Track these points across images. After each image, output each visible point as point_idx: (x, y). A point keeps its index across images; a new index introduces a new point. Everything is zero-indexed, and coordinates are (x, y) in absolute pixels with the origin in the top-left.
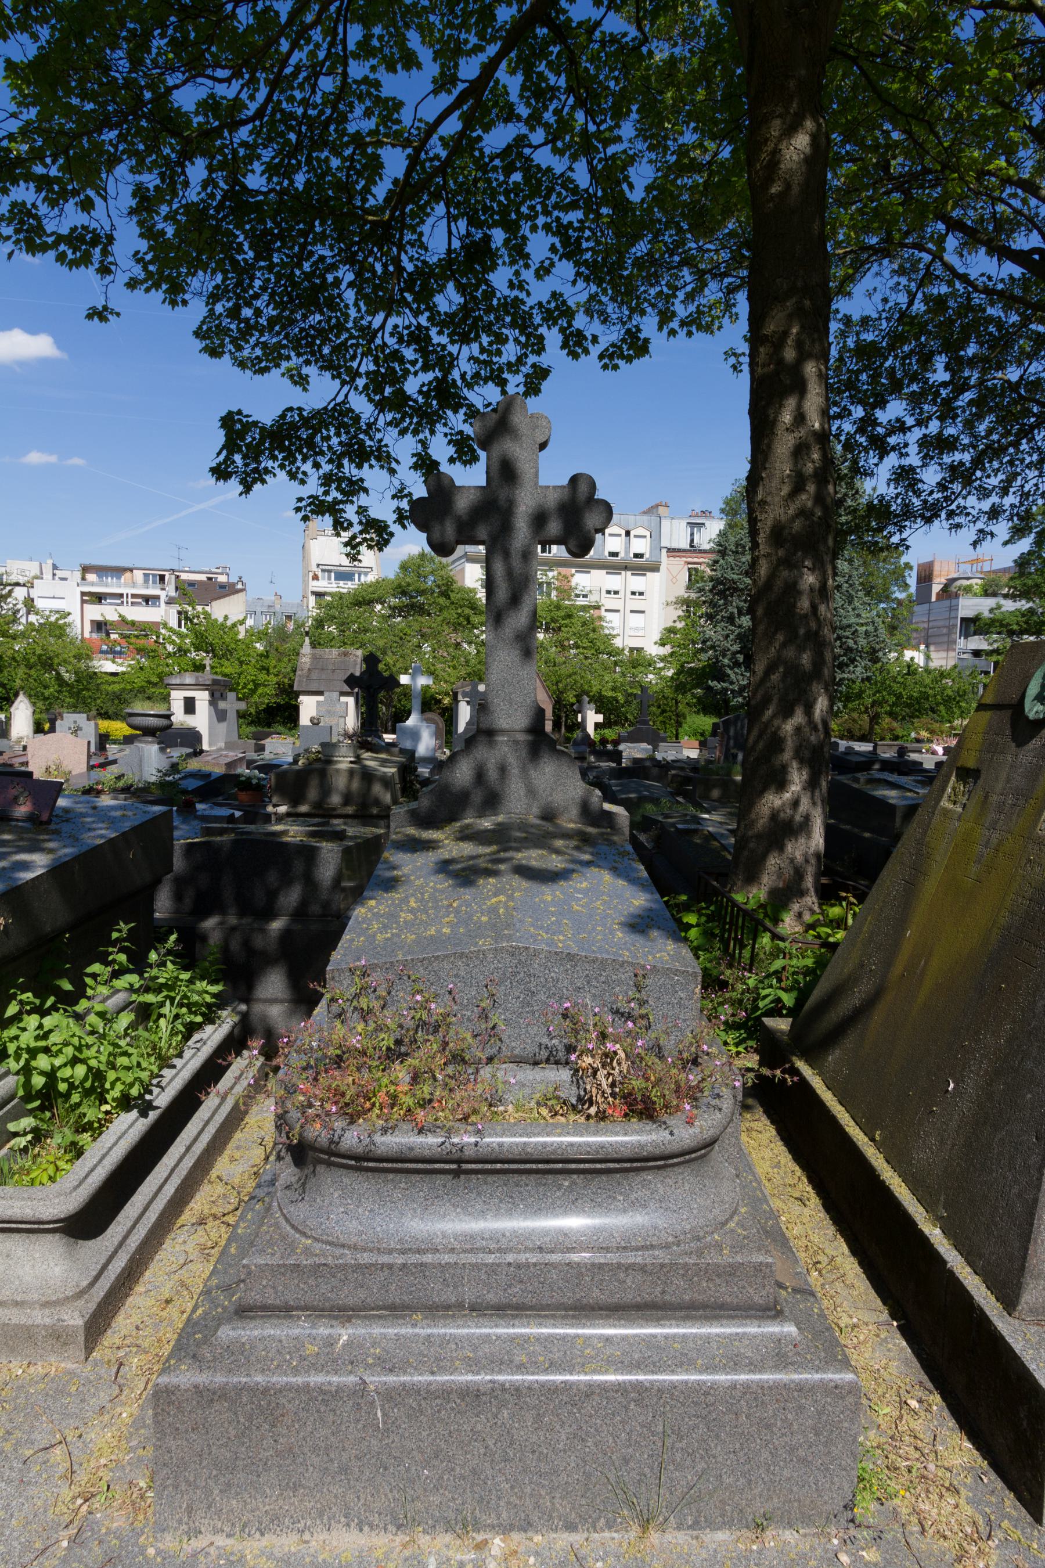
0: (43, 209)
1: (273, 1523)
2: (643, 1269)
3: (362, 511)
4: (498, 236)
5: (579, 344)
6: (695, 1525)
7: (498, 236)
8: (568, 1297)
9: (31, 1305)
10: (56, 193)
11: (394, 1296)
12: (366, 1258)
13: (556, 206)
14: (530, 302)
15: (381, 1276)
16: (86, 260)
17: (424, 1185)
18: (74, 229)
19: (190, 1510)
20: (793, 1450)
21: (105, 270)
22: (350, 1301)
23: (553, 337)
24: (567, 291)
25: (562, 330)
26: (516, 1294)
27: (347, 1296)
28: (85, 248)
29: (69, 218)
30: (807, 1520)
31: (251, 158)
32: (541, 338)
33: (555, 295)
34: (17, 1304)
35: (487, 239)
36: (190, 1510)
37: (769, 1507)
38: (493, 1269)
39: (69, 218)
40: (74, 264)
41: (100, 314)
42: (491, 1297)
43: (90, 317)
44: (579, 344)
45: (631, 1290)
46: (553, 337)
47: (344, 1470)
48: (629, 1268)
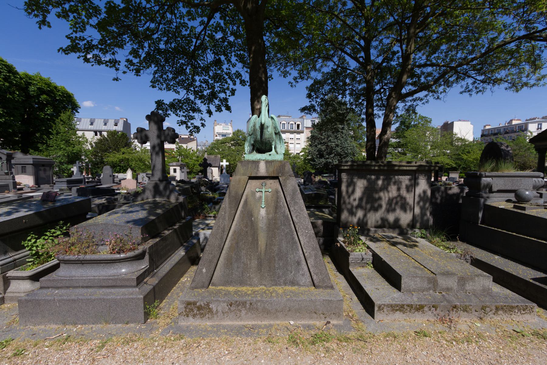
0: (101, 55)
1: (40, 323)
2: (112, 279)
3: (192, 124)
4: (223, 58)
5: (244, 83)
6: (115, 323)
7: (223, 58)
8: (99, 285)
9: (21, 293)
10: (105, 52)
11: (67, 285)
12: (63, 278)
13: (237, 50)
14: (232, 73)
15: (65, 281)
16: (114, 66)
17: (76, 266)
18: (110, 59)
19: (25, 322)
20: (132, 309)
21: (117, 69)
22: (60, 286)
23: (238, 81)
24: (240, 70)
25: (240, 79)
26: (89, 284)
27: (59, 285)
28: (114, 63)
29: (108, 57)
30: (135, 322)
31: (160, 40)
32: (235, 81)
33: (237, 71)
34: (19, 292)
35: (220, 58)
36: (25, 322)
37: (128, 320)
38: (85, 280)
39: (108, 57)
40: (110, 67)
41: (116, 79)
42: (85, 285)
43: (114, 80)
44: (244, 83)
45: (110, 283)
46: (238, 81)
47: (52, 314)
48: (109, 279)
